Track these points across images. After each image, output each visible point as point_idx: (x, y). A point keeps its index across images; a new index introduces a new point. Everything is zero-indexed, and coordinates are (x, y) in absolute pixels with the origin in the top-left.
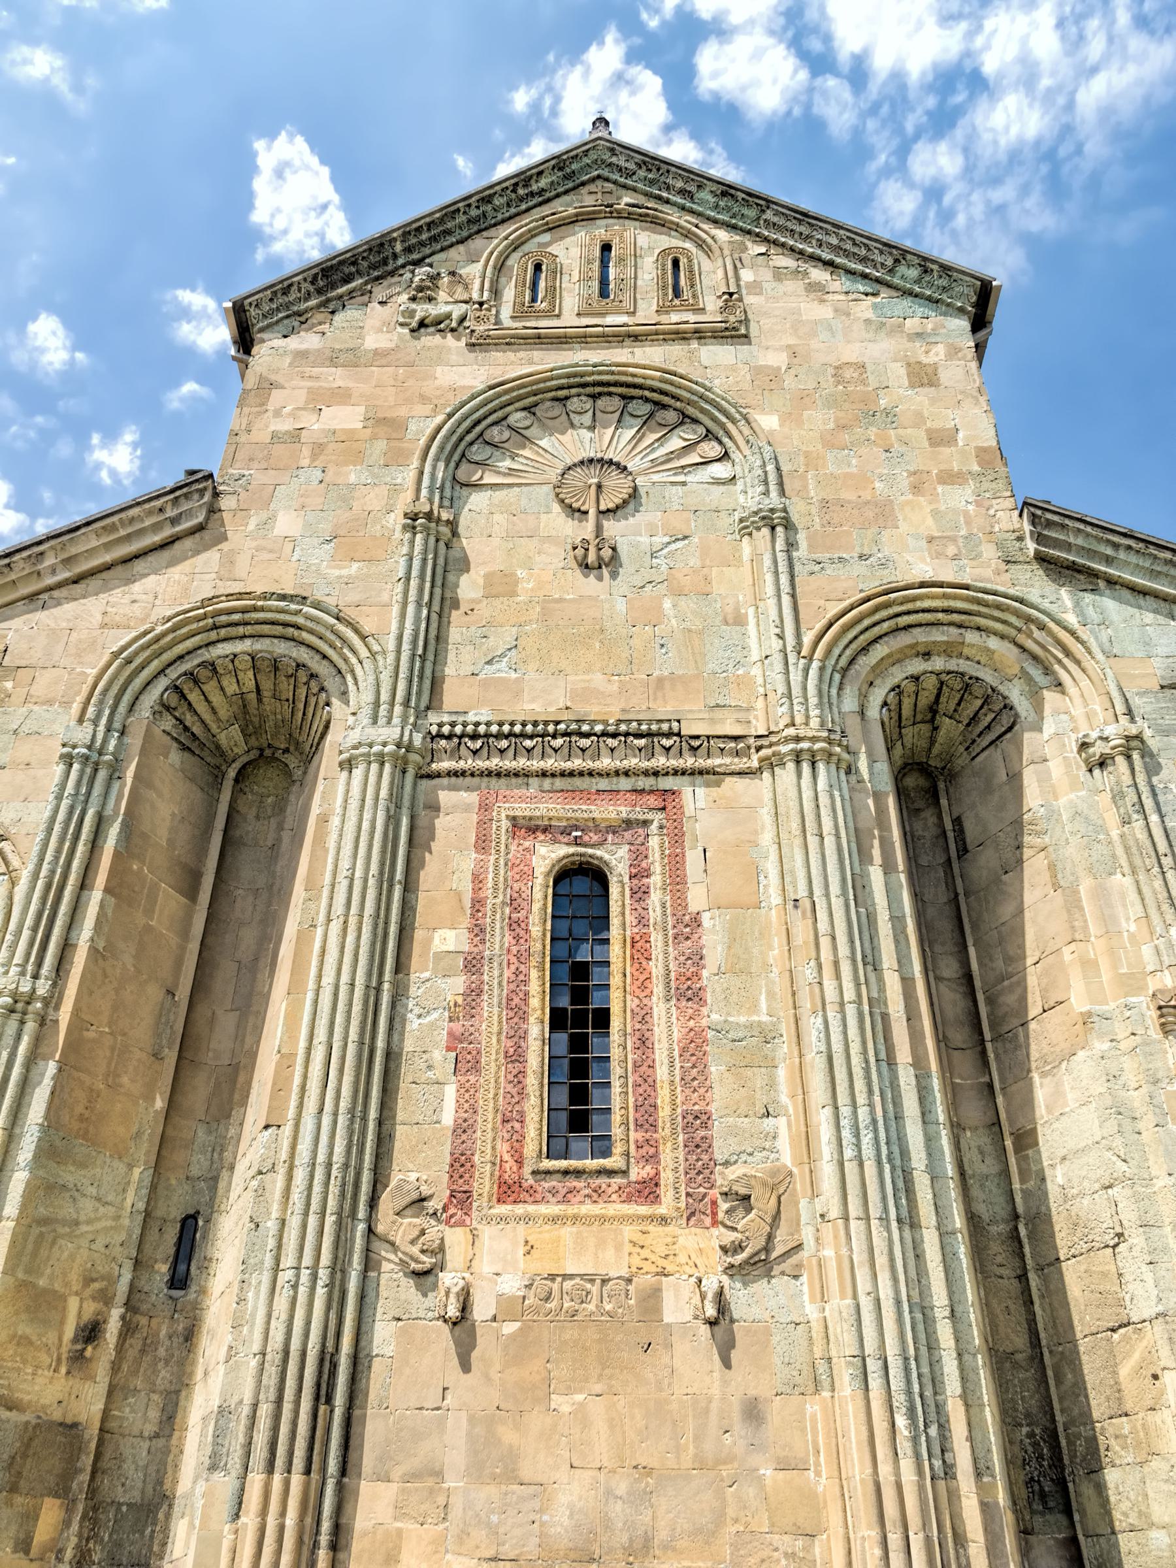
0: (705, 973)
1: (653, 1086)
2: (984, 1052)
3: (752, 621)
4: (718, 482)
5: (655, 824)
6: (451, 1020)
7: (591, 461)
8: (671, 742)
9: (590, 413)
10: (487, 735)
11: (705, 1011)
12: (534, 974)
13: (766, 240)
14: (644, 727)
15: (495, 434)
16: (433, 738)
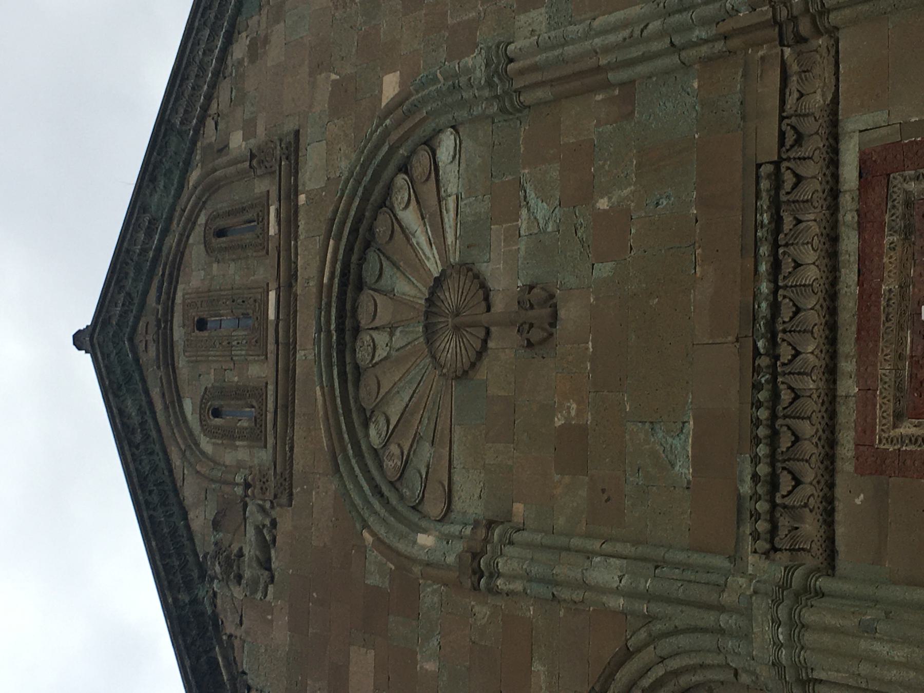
3: (623, 75)
5: (912, 186)
7: (426, 327)
9: (375, 334)
10: (772, 464)
13: (202, 121)
14: (766, 218)
15: (392, 464)
16: (775, 550)
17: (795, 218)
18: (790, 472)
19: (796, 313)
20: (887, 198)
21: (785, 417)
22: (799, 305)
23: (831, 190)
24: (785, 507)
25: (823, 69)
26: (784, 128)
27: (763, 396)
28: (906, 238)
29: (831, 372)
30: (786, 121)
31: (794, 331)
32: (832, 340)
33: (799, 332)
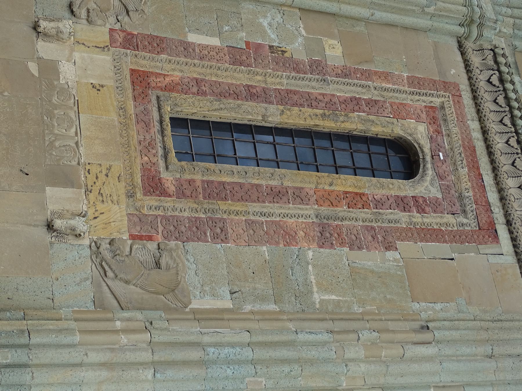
5: (465, 221)
6: (271, 47)
10: (505, 90)
11: (314, 246)
12: (319, 112)
18: (494, 85)
20: (477, 217)
21: (505, 112)
22: (513, 167)
23: (511, 225)
24: (493, 70)
28: (461, 194)
29: (485, 132)
31: (511, 154)
32: (489, 148)
33: (509, 153)
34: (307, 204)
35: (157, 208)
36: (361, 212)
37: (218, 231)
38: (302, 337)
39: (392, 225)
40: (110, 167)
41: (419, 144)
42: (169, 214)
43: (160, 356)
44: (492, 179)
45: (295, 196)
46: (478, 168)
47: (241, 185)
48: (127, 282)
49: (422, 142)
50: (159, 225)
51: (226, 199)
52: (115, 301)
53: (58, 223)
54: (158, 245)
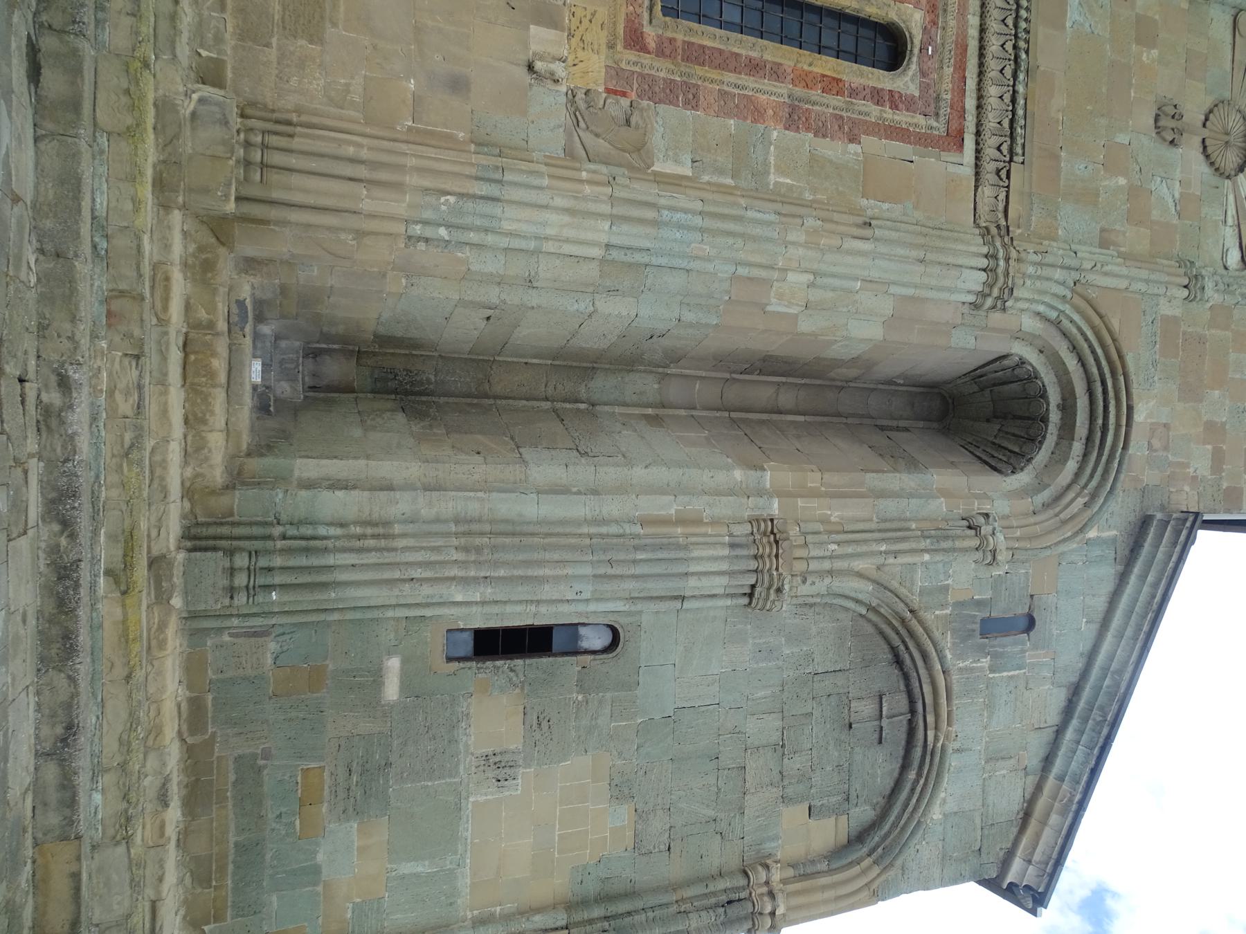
0: (811, 135)
1: (719, 67)
2: (718, 410)
4: (1224, 253)
5: (935, 124)
8: (1005, 152)
11: (780, 127)
14: (1019, 130)
17: (1001, 125)
19: (1003, 69)
21: (1011, 10)
25: (983, 209)
26: (1007, 181)
27: (1023, 25)
28: (939, 95)
29: (982, 30)
30: (1006, 184)
32: (982, 48)
34: (782, 82)
35: (636, 64)
36: (834, 99)
37: (691, 96)
38: (750, 214)
39: (861, 117)
40: (595, 11)
41: (910, 33)
42: (646, 72)
43: (620, 210)
44: (975, 84)
45: (772, 72)
46: (964, 70)
47: (721, 52)
48: (597, 135)
49: (914, 32)
50: (635, 81)
51: (703, 64)
52: (584, 153)
53: (539, 65)
54: (631, 102)
